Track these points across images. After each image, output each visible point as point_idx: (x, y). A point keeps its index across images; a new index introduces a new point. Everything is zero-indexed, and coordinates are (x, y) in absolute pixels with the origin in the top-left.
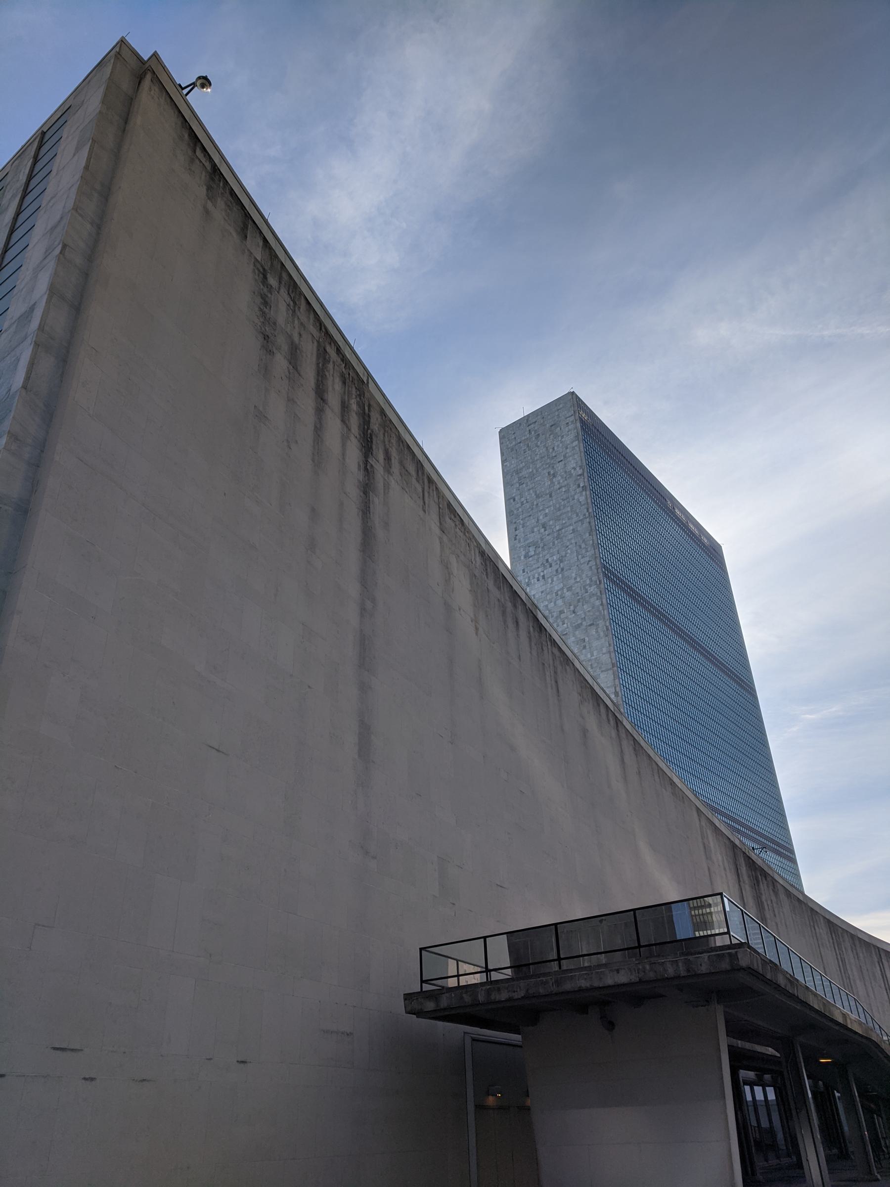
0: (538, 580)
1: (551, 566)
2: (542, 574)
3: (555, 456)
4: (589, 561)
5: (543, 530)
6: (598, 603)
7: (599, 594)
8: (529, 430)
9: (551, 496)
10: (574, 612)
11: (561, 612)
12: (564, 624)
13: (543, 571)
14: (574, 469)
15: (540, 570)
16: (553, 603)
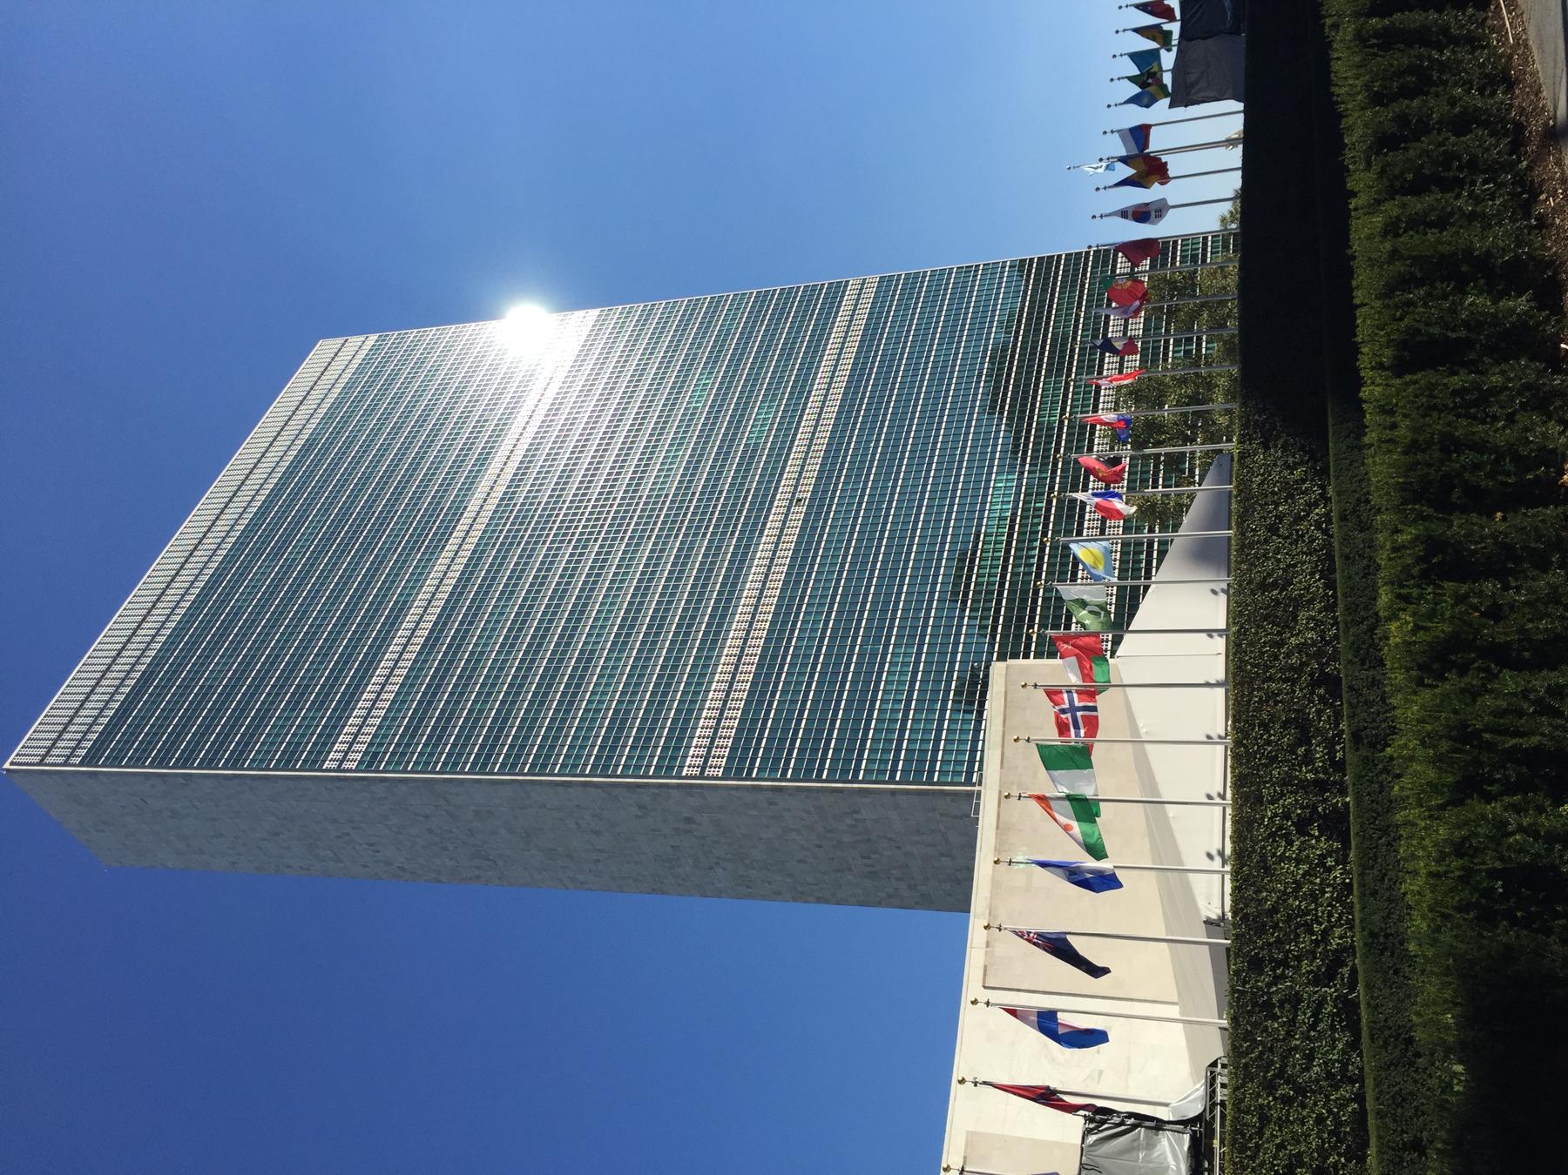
0: (378, 852)
1: (348, 834)
2: (366, 847)
3: (137, 806)
4: (326, 788)
5: (282, 836)
6: (403, 788)
7: (384, 784)
8: (97, 831)
9: (215, 820)
10: (427, 817)
11: (430, 831)
12: (452, 832)
13: (360, 844)
14: (153, 786)
15: (357, 846)
16: (417, 840)
